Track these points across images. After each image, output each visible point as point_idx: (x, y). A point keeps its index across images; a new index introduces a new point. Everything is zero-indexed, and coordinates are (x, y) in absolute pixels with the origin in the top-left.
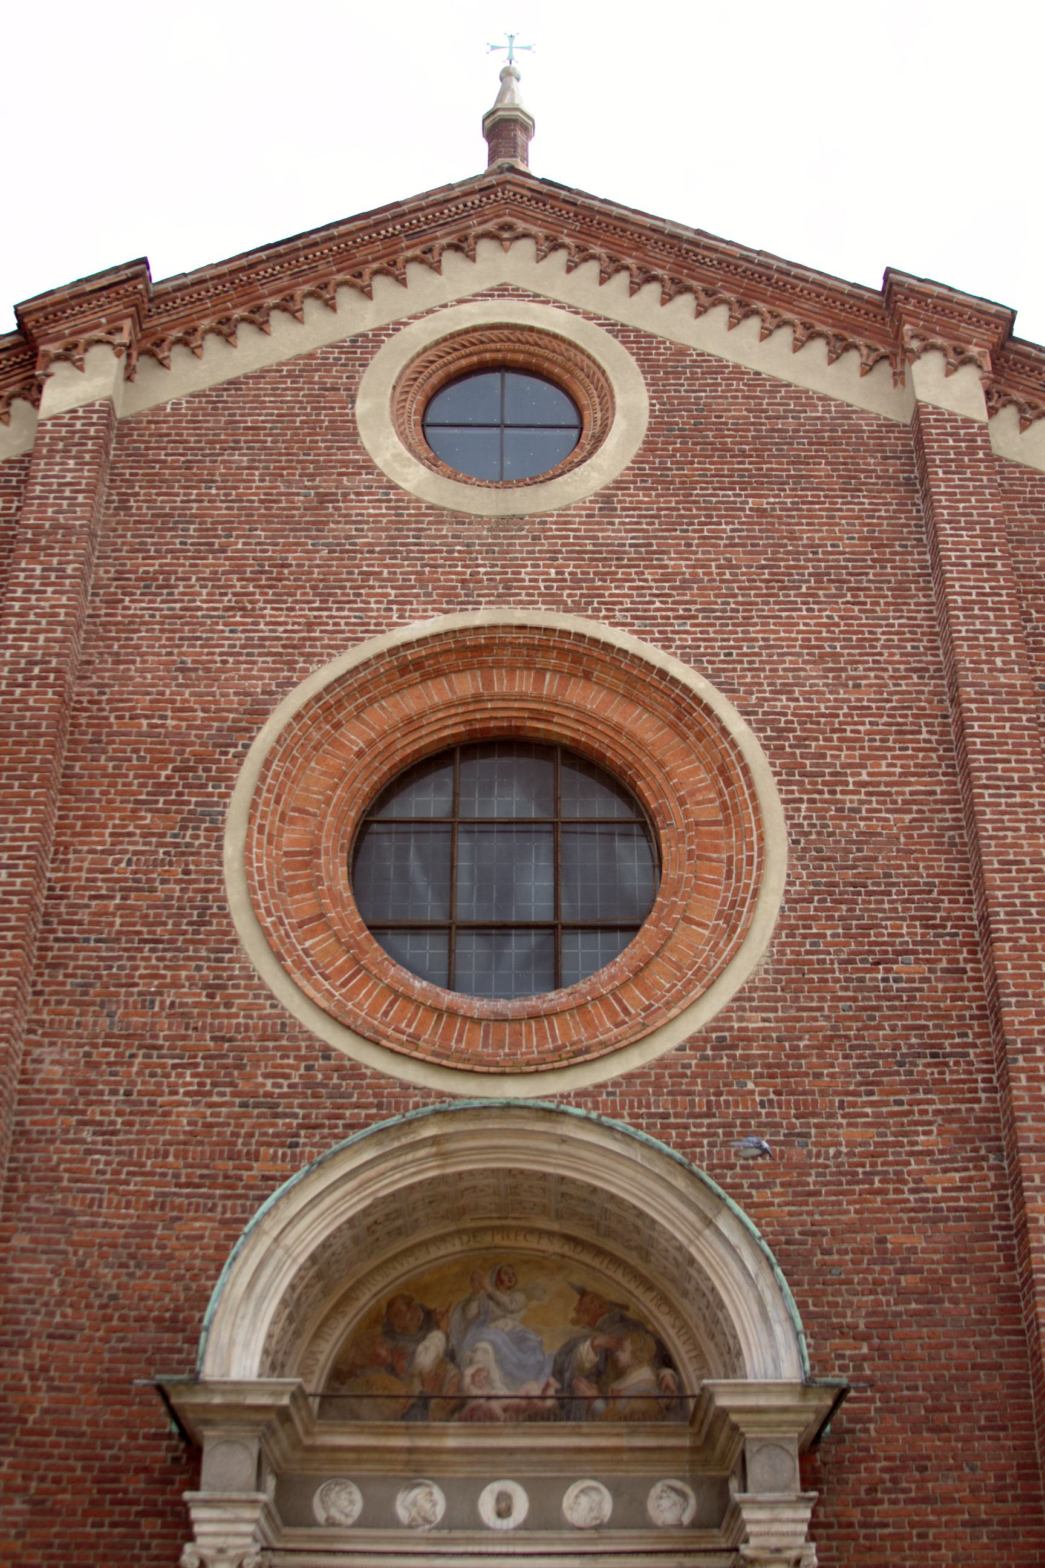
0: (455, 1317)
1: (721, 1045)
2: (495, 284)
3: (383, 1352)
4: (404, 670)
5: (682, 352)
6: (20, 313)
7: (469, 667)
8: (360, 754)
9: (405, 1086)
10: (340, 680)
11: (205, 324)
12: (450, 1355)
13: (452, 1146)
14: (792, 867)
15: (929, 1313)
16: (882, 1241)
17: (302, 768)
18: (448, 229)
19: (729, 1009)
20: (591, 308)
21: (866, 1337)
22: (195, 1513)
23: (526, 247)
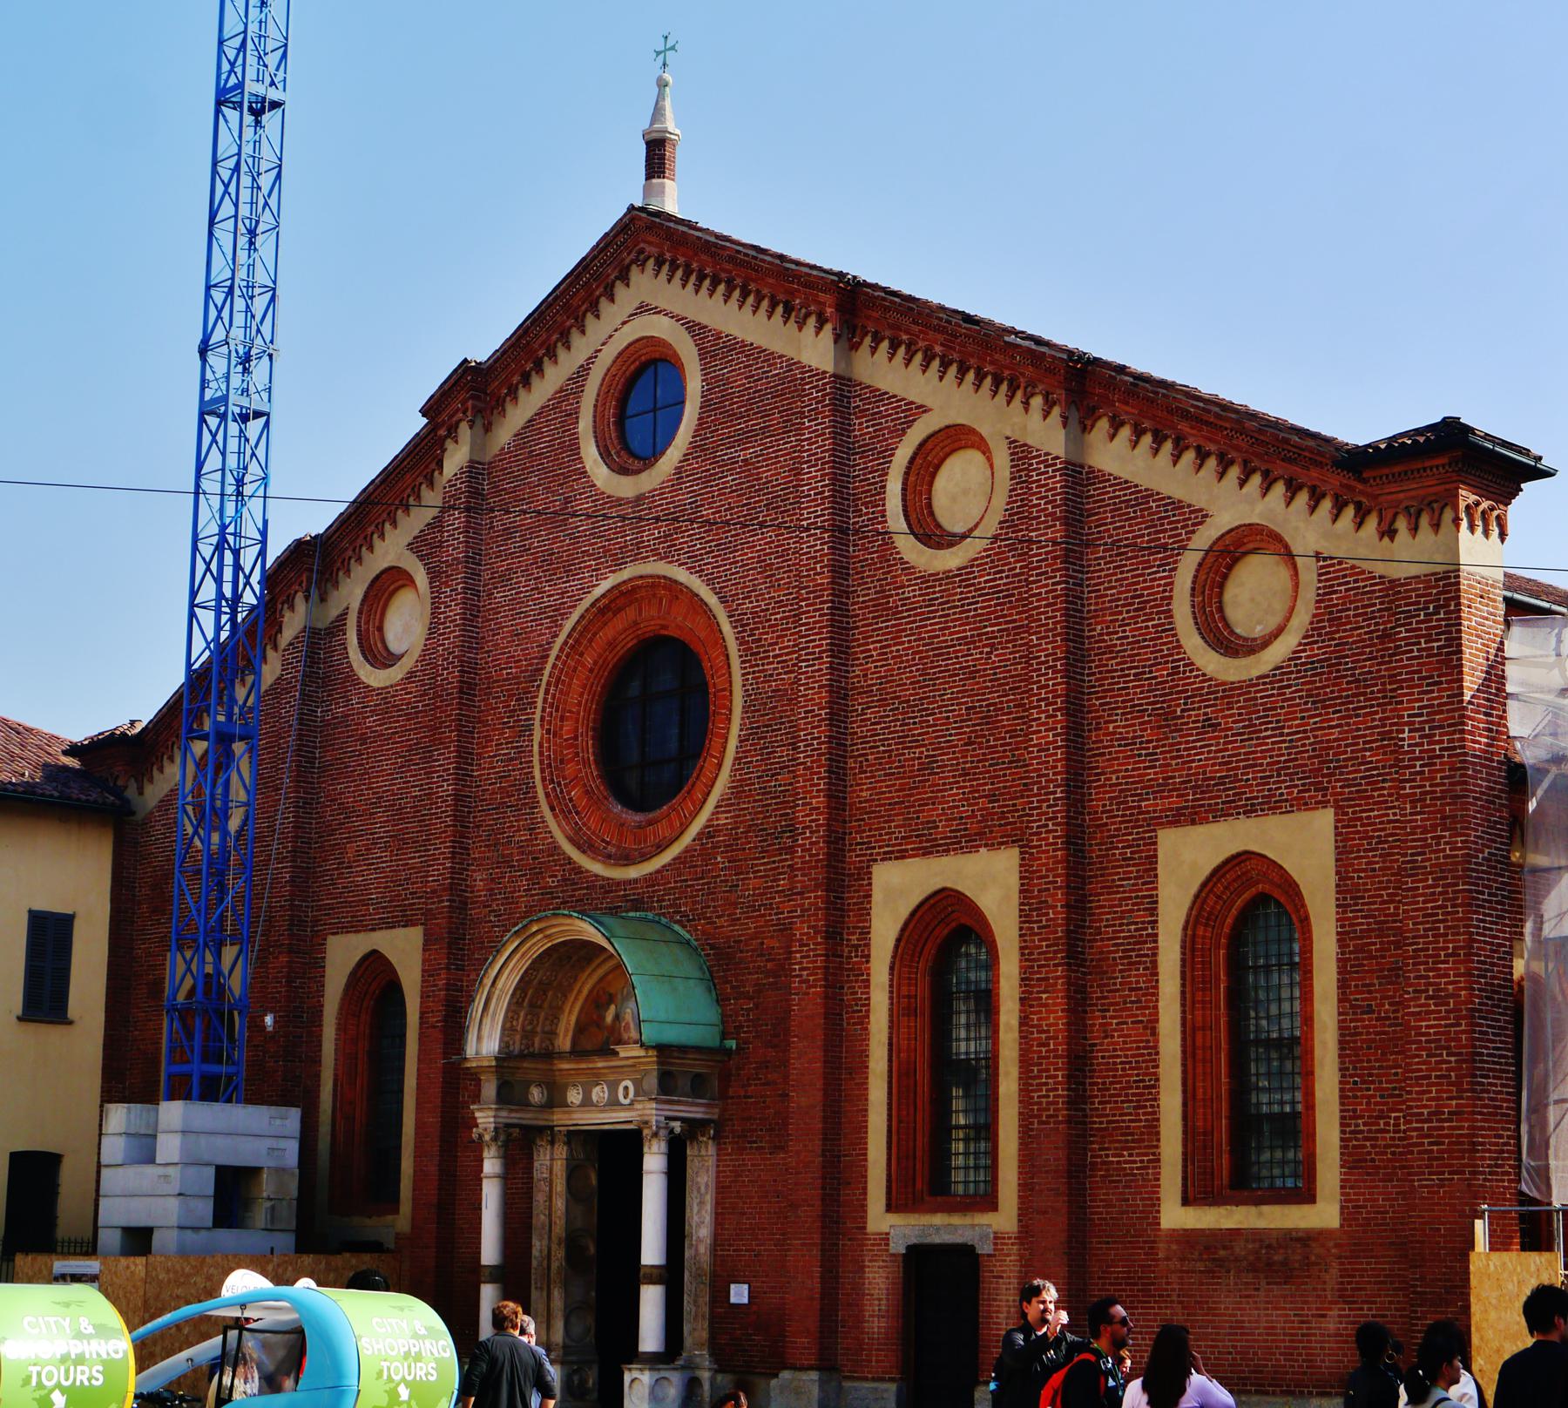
0: (619, 996)
1: (710, 836)
2: (637, 304)
3: (595, 1017)
4: (602, 611)
5: (718, 336)
6: (425, 412)
7: (631, 603)
8: (591, 670)
9: (596, 876)
10: (574, 629)
11: (516, 379)
12: (617, 1017)
13: (548, 933)
14: (743, 719)
15: (776, 983)
16: (762, 943)
17: (570, 685)
18: (613, 266)
19: (713, 814)
20: (677, 311)
21: (751, 998)
22: (477, 1114)
23: (651, 263)
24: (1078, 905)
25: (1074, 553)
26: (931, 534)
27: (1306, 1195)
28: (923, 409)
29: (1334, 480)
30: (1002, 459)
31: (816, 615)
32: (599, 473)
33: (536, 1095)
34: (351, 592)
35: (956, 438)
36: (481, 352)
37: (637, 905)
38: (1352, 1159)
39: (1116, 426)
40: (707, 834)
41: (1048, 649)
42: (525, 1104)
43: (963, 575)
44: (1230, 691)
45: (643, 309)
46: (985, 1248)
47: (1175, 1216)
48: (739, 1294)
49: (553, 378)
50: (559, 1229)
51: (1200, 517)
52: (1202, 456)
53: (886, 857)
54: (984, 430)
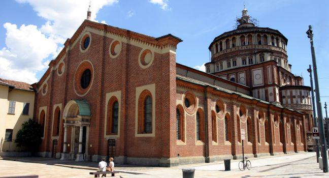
24: (127, 97)
25: (127, 55)
26: (114, 54)
27: (151, 132)
28: (112, 39)
29: (156, 42)
30: (121, 44)
31: (101, 64)
32: (81, 51)
33: (72, 122)
34: (57, 66)
35: (117, 42)
36: (70, 38)
37: (83, 99)
38: (157, 128)
39: (133, 38)
40: (90, 91)
41: (124, 65)
42: (70, 123)
43: (116, 58)
44: (144, 70)
45: (86, 31)
46: (116, 140)
47: (137, 135)
48: (91, 146)
49: (78, 39)
50: (74, 138)
51: (141, 49)
52: (142, 41)
53: (108, 92)
54: (119, 41)
